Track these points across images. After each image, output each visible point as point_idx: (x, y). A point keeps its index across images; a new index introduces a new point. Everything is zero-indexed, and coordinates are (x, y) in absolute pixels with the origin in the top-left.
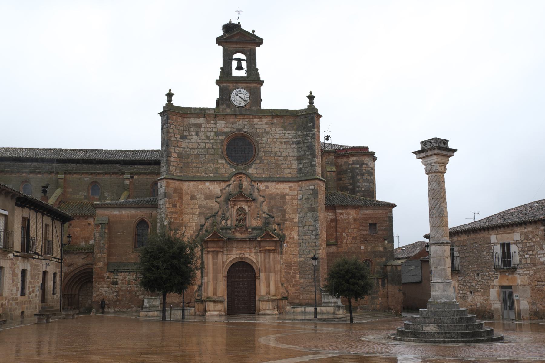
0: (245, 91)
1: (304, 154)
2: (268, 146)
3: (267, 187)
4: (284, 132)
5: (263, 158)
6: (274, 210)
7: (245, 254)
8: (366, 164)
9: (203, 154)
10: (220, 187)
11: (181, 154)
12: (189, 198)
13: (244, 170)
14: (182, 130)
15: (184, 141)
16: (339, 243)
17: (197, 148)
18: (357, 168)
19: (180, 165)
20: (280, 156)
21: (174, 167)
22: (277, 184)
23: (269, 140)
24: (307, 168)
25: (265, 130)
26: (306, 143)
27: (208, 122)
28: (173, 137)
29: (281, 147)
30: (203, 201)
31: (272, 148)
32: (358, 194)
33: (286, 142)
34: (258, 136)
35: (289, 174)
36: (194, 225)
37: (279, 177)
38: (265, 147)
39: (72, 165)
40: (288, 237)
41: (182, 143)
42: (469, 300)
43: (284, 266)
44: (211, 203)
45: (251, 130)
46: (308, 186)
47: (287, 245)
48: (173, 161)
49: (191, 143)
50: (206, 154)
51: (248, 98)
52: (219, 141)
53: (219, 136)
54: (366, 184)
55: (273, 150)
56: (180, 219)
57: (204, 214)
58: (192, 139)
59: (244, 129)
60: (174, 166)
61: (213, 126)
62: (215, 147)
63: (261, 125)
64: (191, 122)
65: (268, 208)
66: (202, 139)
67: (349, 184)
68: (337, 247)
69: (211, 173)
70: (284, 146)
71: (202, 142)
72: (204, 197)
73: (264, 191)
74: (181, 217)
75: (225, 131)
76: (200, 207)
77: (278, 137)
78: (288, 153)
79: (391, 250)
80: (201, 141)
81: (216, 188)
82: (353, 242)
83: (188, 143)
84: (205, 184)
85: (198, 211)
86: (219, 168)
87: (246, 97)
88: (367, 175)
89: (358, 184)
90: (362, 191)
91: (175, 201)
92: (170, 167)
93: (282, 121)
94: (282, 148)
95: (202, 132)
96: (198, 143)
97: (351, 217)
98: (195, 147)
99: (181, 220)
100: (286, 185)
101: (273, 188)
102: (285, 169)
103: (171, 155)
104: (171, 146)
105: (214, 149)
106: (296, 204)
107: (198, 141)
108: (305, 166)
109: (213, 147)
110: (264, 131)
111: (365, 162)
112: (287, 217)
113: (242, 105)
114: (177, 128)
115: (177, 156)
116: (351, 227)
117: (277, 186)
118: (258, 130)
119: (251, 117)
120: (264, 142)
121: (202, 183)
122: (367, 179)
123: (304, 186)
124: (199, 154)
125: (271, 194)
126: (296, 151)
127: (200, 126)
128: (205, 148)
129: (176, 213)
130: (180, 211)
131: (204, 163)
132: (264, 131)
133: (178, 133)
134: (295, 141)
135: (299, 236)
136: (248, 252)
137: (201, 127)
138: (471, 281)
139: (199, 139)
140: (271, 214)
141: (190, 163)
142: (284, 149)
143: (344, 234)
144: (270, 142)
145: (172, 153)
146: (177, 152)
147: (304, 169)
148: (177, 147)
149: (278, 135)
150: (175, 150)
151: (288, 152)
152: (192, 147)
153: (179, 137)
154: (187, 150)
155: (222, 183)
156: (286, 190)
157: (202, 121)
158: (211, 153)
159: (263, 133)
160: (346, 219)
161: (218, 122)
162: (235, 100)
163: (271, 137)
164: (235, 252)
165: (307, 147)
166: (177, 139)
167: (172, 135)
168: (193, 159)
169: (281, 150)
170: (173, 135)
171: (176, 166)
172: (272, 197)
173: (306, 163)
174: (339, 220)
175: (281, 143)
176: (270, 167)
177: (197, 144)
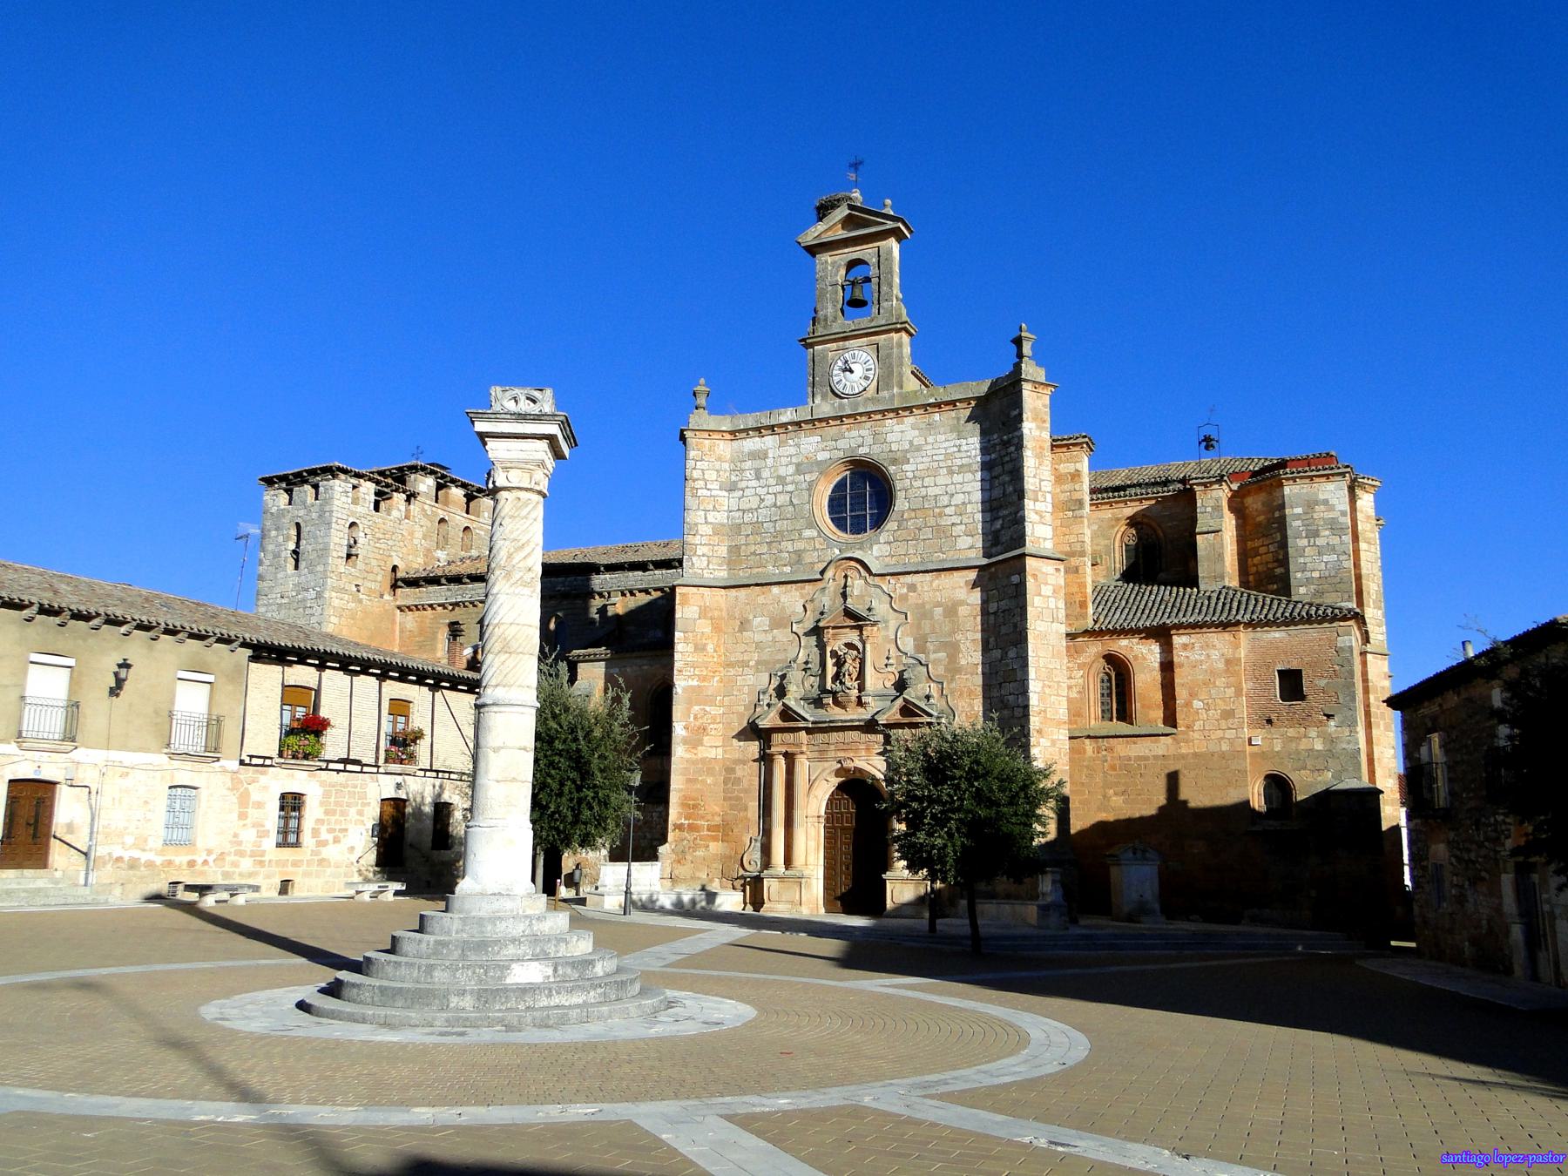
0: (865, 354)
1: (1004, 493)
2: (917, 484)
3: (912, 588)
4: (958, 442)
6: (928, 644)
8: (1326, 502)
10: (802, 596)
11: (723, 525)
12: (737, 630)
13: (860, 549)
14: (725, 471)
16: (1183, 729)
18: (1298, 517)
19: (719, 552)
20: (947, 506)
21: (705, 558)
22: (937, 578)
23: (921, 467)
24: (1010, 528)
25: (911, 442)
26: (1008, 462)
27: (782, 444)
28: (702, 488)
31: (926, 487)
32: (1302, 590)
33: (960, 467)
34: (894, 461)
35: (969, 549)
37: (943, 560)
39: (636, 573)
40: (964, 715)
42: (1470, 907)
44: (783, 635)
45: (876, 449)
46: (1008, 577)
48: (701, 544)
49: (744, 499)
51: (871, 369)
52: (804, 486)
53: (804, 474)
54: (1325, 558)
55: (932, 491)
56: (716, 679)
58: (747, 487)
59: (861, 448)
60: (703, 555)
61: (792, 450)
62: (795, 501)
63: (902, 432)
64: (746, 450)
67: (1276, 564)
68: (1177, 742)
69: (785, 565)
70: (957, 478)
73: (904, 598)
74: (717, 674)
75: (819, 459)
76: (758, 645)
77: (942, 457)
79: (1351, 746)
81: (792, 600)
82: (1223, 724)
86: (805, 550)
87: (867, 370)
88: (1327, 533)
89: (1302, 560)
90: (1309, 581)
91: (701, 637)
92: (694, 559)
93: (953, 414)
94: (952, 483)
95: (767, 470)
97: (1215, 654)
100: (960, 580)
101: (926, 589)
102: (959, 536)
103: (697, 530)
110: (907, 447)
111: (1321, 497)
112: (963, 662)
113: (857, 391)
114: (714, 466)
116: (1217, 683)
117: (936, 583)
118: (894, 447)
119: (879, 417)
120: (908, 473)
122: (1327, 544)
124: (762, 523)
125: (923, 605)
127: (761, 455)
128: (775, 505)
129: (706, 665)
131: (771, 542)
132: (907, 447)
133: (715, 478)
136: (863, 753)
137: (767, 457)
138: (1467, 845)
140: (922, 657)
142: (957, 486)
143: (1197, 704)
144: (923, 472)
146: (711, 523)
148: (713, 510)
149: (943, 451)
150: (706, 518)
151: (969, 493)
152: (747, 506)
153: (718, 488)
154: (737, 514)
156: (957, 591)
157: (770, 441)
158: (788, 516)
159: (906, 451)
160: (1201, 661)
161: (804, 440)
162: (841, 380)
163: (924, 459)
164: (832, 754)
165: (1011, 472)
166: (714, 493)
167: (701, 483)
168: (748, 535)
169: (951, 489)
170: (701, 483)
172: (924, 613)
173: (1007, 516)
174: (1181, 666)
175: (951, 472)
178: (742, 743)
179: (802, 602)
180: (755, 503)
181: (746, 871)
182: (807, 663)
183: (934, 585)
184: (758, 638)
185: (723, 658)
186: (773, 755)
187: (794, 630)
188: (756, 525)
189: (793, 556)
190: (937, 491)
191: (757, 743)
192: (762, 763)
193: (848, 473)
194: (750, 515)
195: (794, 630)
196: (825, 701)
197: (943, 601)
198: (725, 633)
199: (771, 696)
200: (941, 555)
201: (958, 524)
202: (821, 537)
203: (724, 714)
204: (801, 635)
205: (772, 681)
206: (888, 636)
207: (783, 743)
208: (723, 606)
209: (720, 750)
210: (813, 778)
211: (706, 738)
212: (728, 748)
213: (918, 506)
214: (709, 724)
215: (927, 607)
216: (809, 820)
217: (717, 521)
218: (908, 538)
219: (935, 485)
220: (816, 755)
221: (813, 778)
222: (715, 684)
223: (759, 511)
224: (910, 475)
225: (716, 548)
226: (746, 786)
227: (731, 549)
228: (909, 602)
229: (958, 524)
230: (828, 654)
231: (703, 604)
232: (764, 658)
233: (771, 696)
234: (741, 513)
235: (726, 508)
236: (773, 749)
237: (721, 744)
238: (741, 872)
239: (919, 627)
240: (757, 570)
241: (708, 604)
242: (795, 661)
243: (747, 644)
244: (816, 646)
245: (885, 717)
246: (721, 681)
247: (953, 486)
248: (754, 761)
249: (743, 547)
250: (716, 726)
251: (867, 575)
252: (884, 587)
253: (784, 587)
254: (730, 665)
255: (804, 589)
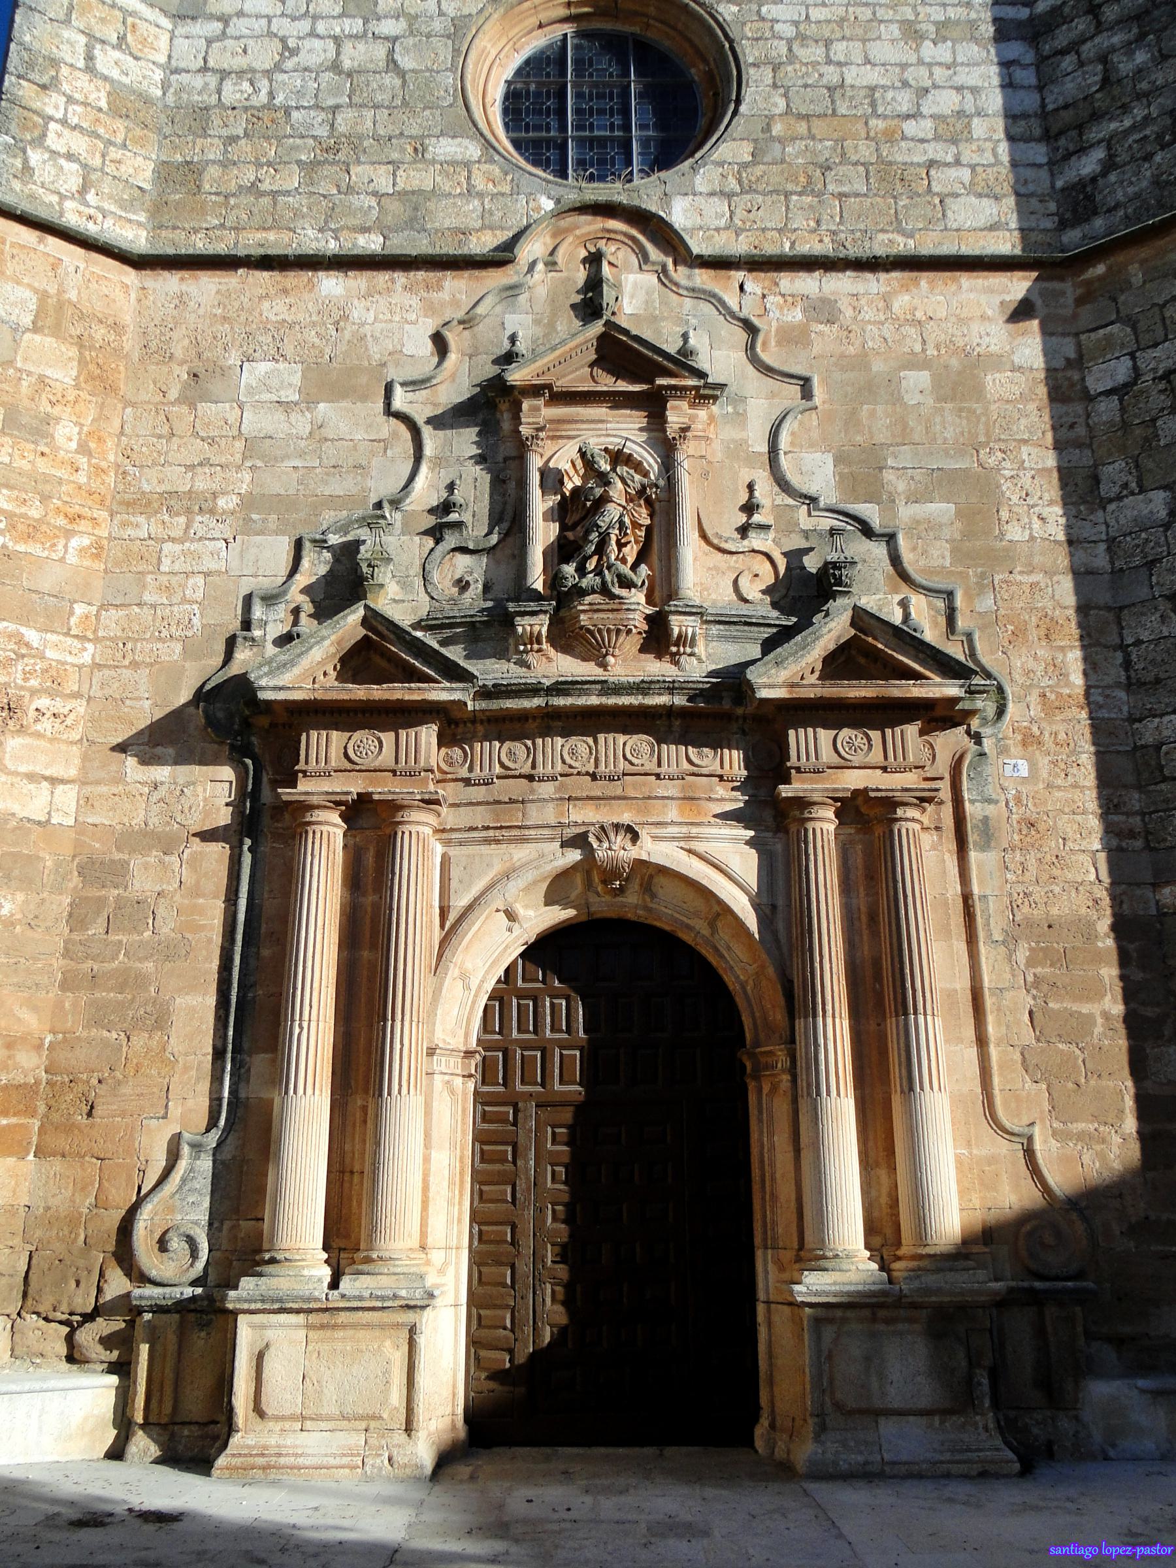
2: (815, 53)
5: (777, 129)
7: (643, 833)
9: (317, 107)
10: (430, 309)
11: (147, 101)
12: (173, 394)
15: (180, 31)
17: (278, 68)
20: (908, 117)
29: (913, 59)
30: (285, 406)
36: (199, 595)
38: (792, 56)
40: (1033, 698)
41: (166, 37)
43: (1022, 955)
47: (1033, 767)
48: (64, 122)
49: (229, 43)
50: (337, 107)
56: (75, 542)
57: (280, 504)
60: (70, 157)
62: (406, 62)
65: (837, 461)
66: (315, 18)
69: (365, 230)
71: (313, 34)
72: (297, 379)
73: (794, 337)
74: (83, 526)
78: (969, 96)
80: (304, 26)
83: (209, 42)
84: (311, 286)
85: (244, 482)
86: (434, 192)
94: (921, 62)
96: (283, 40)
98: (257, 65)
99: (82, 551)
100: (983, 299)
102: (957, 195)
104: (67, 21)
105: (402, 74)
106: (1081, 431)
107: (282, 26)
108: (1123, 157)
109: (392, 63)
115: (103, 104)
117: (901, 302)
120: (777, 27)
121: (294, 278)
123: (1137, 278)
124: (287, 111)
125: (861, 361)
126: (1033, 81)
128: (335, 67)
130: (82, 478)
134: (1019, 24)
135: (1130, 686)
136: (672, 813)
139: (294, 19)
140: (870, 512)
141: (214, 162)
145: (65, 71)
147: (1112, 177)
150: (90, 58)
154: (198, 82)
155: (447, 284)
158: (379, 97)
164: (549, 814)
168: (233, 139)
171: (85, 166)
176: (839, 182)
177: (276, 45)
178: (162, 773)
179: (429, 326)
180: (264, 56)
181: (143, 1279)
182: (446, 507)
183: (896, 306)
184: (253, 422)
185: (111, 479)
186: (305, 807)
187: (398, 403)
188: (266, 115)
189: (394, 206)
190: (872, 76)
191: (227, 773)
192: (248, 842)
193: (569, 29)
194: (246, 85)
195: (398, 403)
196: (524, 625)
197: (933, 351)
198: (128, 403)
199: (296, 611)
200: (900, 239)
201: (947, 165)
202: (491, 161)
203: (99, 666)
204: (420, 420)
205: (305, 563)
206: (742, 444)
207: (351, 765)
208: (127, 318)
209: (67, 797)
210: (460, 902)
211: (14, 743)
212: (103, 789)
213: (819, 110)
214: (34, 692)
215: (878, 366)
216: (441, 1063)
217: (126, 80)
218: (790, 187)
219: (867, 61)
220: (480, 817)
221: (460, 902)
222: (72, 558)
223: (280, 77)
224: (788, 31)
225: (114, 153)
226: (167, 928)
227: (165, 173)
228: (817, 349)
229: (947, 165)
230: (535, 478)
231: (52, 290)
232: (276, 488)
233: (296, 611)
234: (212, 80)
235: (162, 59)
236: (303, 786)
237: (73, 772)
238: (117, 1284)
239: (851, 421)
240: (260, 236)
241: (73, 295)
242: (395, 503)
243: (212, 441)
244: (481, 459)
245: (783, 675)
246: (97, 551)
247: (923, 71)
248: (207, 836)
249: (213, 171)
250: (59, 706)
251: (669, 261)
252: (726, 298)
253: (359, 281)
254: (141, 504)
255: (440, 288)
